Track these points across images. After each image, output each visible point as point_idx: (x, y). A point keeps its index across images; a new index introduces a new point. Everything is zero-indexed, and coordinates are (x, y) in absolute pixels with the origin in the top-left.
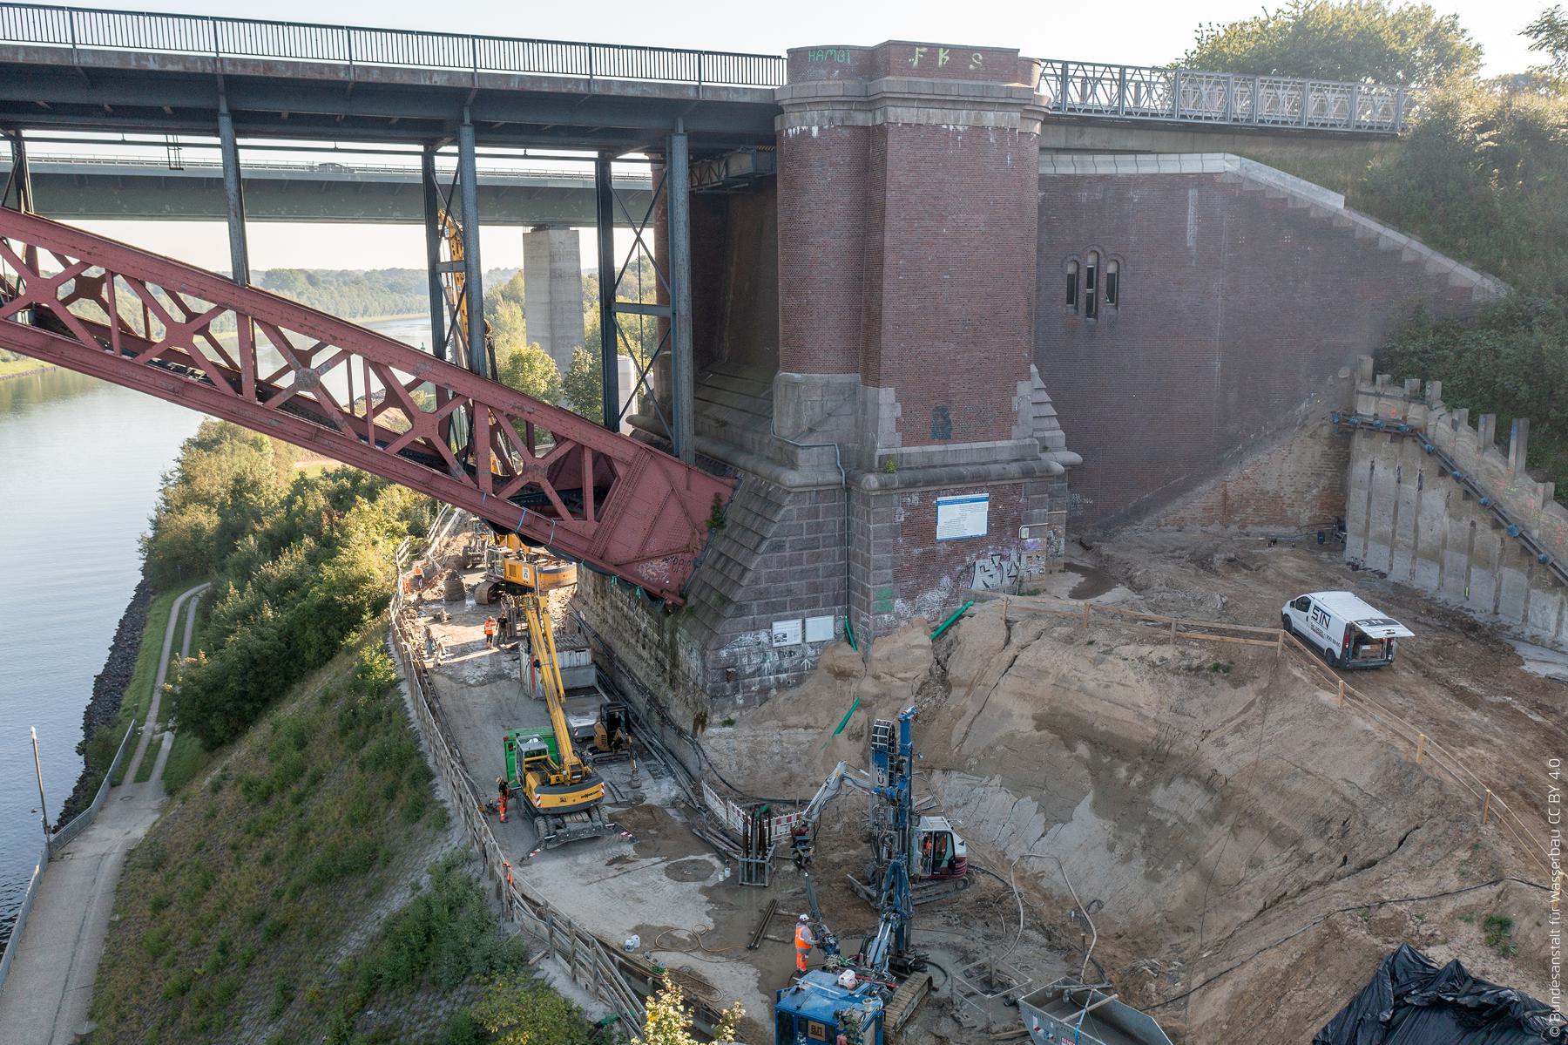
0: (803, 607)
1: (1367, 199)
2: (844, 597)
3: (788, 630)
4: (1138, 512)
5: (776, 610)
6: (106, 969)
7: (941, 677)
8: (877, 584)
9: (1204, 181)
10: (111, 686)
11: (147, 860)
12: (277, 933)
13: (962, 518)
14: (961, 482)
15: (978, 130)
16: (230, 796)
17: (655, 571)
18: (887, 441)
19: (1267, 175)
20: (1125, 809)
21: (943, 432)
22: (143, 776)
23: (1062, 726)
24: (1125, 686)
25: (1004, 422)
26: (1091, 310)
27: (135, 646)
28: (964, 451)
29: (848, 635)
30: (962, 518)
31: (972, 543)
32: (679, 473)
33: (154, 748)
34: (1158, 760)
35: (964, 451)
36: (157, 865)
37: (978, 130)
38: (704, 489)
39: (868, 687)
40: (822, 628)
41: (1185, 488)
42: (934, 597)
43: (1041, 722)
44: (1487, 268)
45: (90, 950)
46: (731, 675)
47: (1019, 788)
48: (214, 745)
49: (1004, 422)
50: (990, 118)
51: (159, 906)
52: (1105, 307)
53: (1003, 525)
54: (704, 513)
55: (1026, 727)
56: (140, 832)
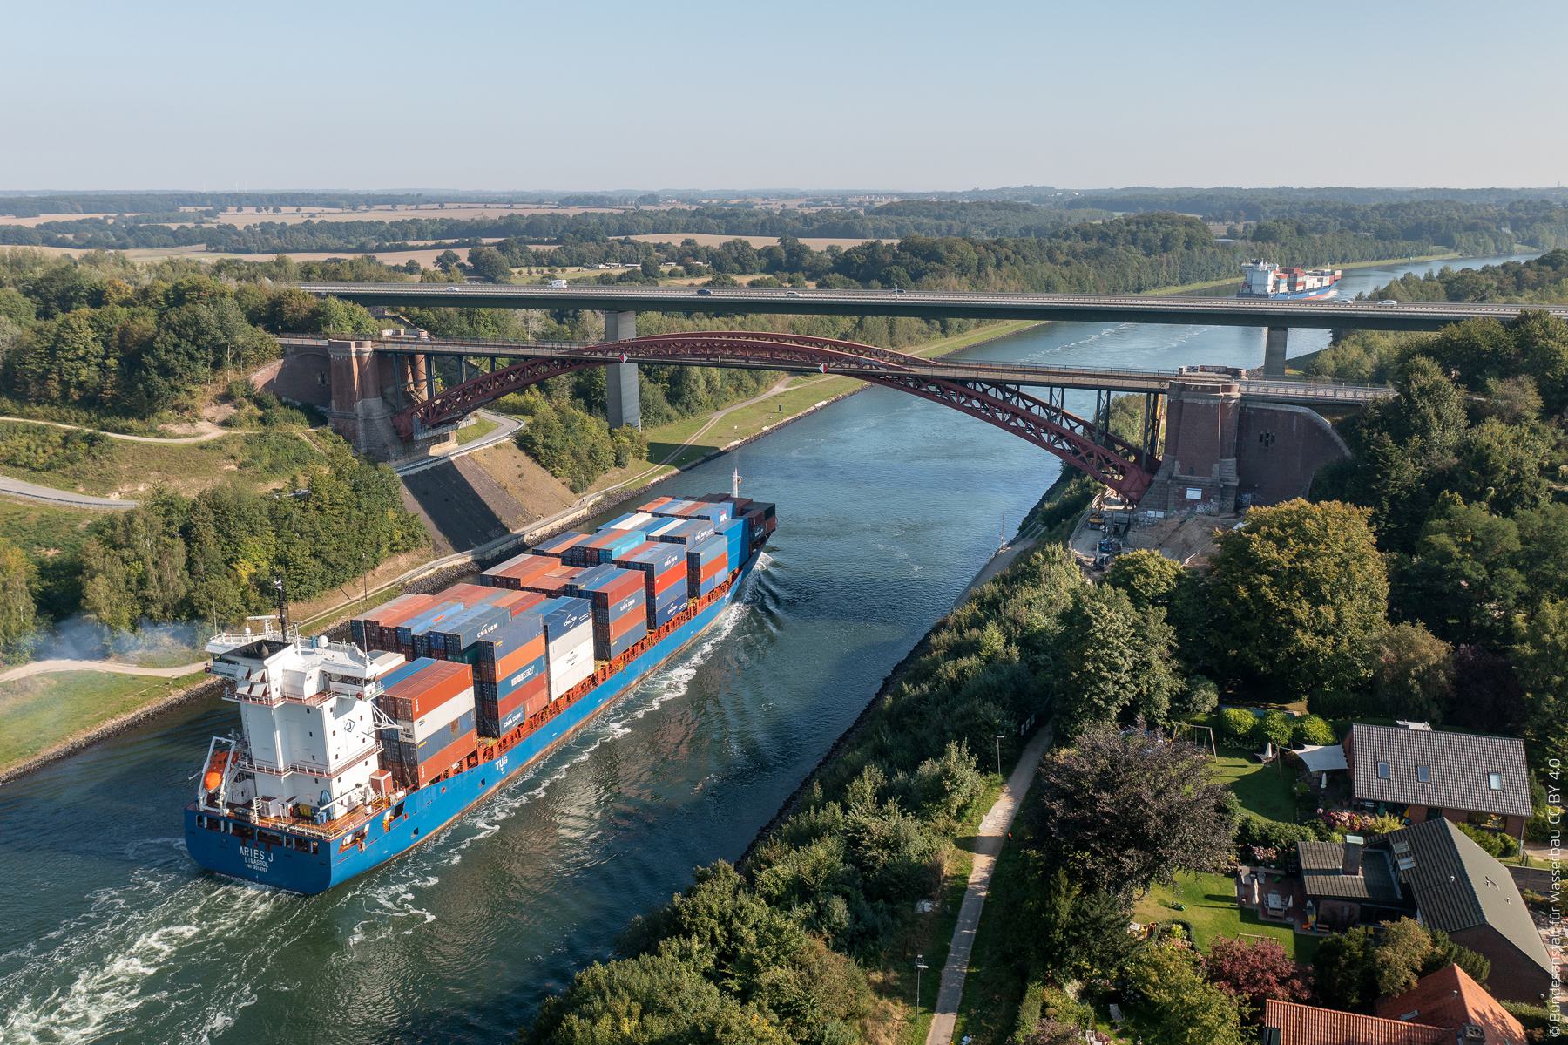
2: (1165, 509)
3: (1151, 513)
8: (1171, 506)
10: (1033, 512)
13: (1194, 494)
14: (1195, 486)
15: (1208, 405)
17: (1133, 494)
19: (1315, 415)
21: (1192, 472)
28: (1197, 478)
29: (1166, 518)
30: (1194, 494)
35: (1197, 478)
37: (1208, 405)
38: (1147, 477)
40: (1160, 514)
53: (1205, 498)
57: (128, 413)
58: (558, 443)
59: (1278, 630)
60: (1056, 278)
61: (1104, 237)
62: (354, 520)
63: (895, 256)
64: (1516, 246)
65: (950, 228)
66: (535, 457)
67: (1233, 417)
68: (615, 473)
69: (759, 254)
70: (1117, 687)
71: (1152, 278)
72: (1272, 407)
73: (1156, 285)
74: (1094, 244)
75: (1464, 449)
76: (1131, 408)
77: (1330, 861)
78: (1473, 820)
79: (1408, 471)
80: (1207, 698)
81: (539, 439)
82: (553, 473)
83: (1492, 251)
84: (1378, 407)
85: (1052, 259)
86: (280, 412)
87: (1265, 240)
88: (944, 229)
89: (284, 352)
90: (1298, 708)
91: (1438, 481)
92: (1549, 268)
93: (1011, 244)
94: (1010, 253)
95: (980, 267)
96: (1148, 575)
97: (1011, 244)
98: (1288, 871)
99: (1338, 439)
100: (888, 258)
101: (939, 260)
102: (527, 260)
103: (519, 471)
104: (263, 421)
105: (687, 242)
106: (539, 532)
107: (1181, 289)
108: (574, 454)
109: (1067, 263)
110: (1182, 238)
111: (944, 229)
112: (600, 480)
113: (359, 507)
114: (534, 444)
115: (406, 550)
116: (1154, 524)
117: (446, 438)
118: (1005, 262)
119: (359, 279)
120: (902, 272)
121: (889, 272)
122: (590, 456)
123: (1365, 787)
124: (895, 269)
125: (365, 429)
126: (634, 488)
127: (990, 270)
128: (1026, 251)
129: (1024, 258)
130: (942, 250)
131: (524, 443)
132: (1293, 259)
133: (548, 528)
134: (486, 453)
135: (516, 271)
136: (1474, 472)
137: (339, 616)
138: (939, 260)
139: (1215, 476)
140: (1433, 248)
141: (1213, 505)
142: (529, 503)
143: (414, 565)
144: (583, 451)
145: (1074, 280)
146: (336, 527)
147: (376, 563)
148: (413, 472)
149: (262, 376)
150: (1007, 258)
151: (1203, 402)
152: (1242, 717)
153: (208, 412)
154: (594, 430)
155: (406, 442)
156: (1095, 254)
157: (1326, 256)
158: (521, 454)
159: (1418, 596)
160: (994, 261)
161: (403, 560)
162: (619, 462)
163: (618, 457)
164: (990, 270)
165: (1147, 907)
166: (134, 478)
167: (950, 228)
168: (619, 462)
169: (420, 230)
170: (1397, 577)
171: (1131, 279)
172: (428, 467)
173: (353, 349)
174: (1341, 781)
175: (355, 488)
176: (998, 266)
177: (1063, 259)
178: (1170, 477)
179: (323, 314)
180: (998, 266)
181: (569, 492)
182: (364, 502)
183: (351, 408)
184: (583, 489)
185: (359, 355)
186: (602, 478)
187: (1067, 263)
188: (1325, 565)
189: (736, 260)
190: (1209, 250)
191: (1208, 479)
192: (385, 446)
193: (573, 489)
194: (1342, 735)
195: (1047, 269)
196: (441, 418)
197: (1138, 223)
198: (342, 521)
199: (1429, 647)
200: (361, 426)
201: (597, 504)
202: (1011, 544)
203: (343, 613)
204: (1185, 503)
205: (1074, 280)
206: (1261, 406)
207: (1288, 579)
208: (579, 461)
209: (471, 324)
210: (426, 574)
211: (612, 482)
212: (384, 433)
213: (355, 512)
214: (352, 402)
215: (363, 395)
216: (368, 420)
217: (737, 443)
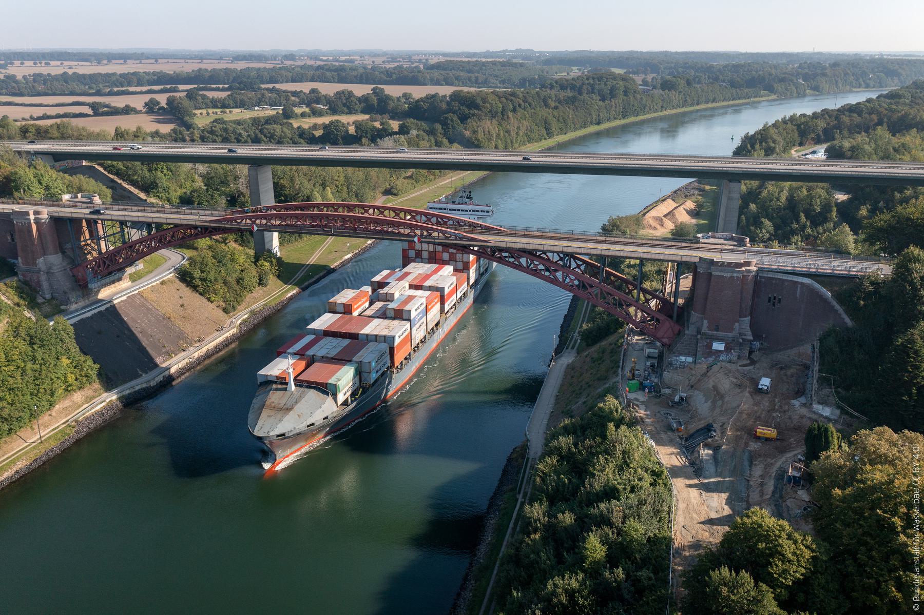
0: (687, 355)
1: (838, 297)
2: (695, 355)
3: (683, 358)
4: (780, 350)
5: (681, 354)
6: (562, 385)
7: (705, 375)
9: (802, 284)
11: (571, 368)
12: (589, 386)
13: (718, 346)
14: (719, 340)
16: (588, 359)
17: (665, 340)
18: (705, 329)
19: (817, 285)
20: (714, 402)
21: (717, 330)
22: (573, 348)
23: (715, 388)
24: (725, 384)
25: (731, 330)
26: (774, 304)
27: (576, 307)
28: (721, 334)
29: (695, 362)
30: (718, 346)
31: (720, 351)
32: (672, 324)
33: (576, 341)
34: (722, 397)
36: (573, 369)
37: (732, 277)
39: (694, 372)
40: (690, 359)
41: (792, 348)
42: (711, 359)
43: (713, 387)
44: (852, 320)
45: (559, 382)
46: (671, 364)
47: (705, 395)
48: (589, 346)
49: (731, 330)
50: (735, 275)
51: (572, 377)
52: (778, 306)
53: (728, 349)
54: (676, 332)
55: (711, 386)
56: (570, 361)
58: (212, 276)
60: (550, 117)
61: (573, 87)
62: (29, 372)
63: (448, 104)
64: (808, 91)
65: (477, 78)
66: (194, 288)
67: (751, 287)
68: (258, 291)
69: (360, 100)
71: (607, 115)
72: (780, 276)
73: (609, 120)
74: (569, 93)
76: (622, 228)
81: (197, 274)
82: (209, 299)
84: (872, 283)
85: (547, 105)
88: (473, 79)
92: (855, 115)
93: (521, 95)
94: (521, 102)
95: (503, 112)
96: (784, 559)
97: (521, 95)
99: (837, 307)
100: (444, 106)
101: (477, 107)
102: (206, 104)
103: (181, 302)
105: (313, 91)
106: (196, 355)
107: (623, 122)
108: (225, 282)
109: (556, 108)
110: (622, 89)
111: (473, 79)
112: (247, 299)
113: (34, 359)
114: (193, 278)
115: (80, 388)
116: (684, 366)
117: (120, 279)
118: (518, 109)
119: (64, 137)
120: (455, 118)
121: (446, 118)
122: (238, 282)
124: (450, 115)
125: (48, 280)
126: (273, 304)
127: (510, 114)
128: (530, 100)
129: (530, 104)
130: (479, 101)
131: (184, 276)
132: (686, 101)
133: (204, 350)
134: (153, 290)
135: (198, 112)
137: (14, 462)
138: (477, 107)
139: (735, 333)
140: (762, 92)
141: (734, 354)
142: (189, 329)
143: (89, 399)
144: (232, 280)
145: (561, 119)
146: (11, 381)
147: (52, 405)
148: (89, 314)
150: (520, 105)
151: (729, 275)
154: (242, 259)
155: (83, 287)
156: (571, 101)
157: (704, 99)
158: (182, 286)
160: (511, 107)
161: (78, 396)
162: (261, 282)
163: (260, 280)
164: (510, 114)
167: (477, 78)
168: (261, 282)
171: (594, 117)
172: (103, 308)
173: (32, 217)
175: (31, 344)
176: (514, 110)
177: (553, 104)
178: (699, 332)
179: (14, 181)
180: (514, 110)
181: (222, 314)
182: (39, 354)
183: (35, 264)
184: (234, 309)
185: (37, 221)
186: (249, 297)
187: (556, 108)
189: (344, 105)
190: (638, 97)
191: (730, 335)
192: (65, 293)
193: (225, 311)
195: (544, 112)
196: (111, 267)
197: (593, 79)
198: (18, 375)
200: (43, 278)
201: (244, 321)
202: (559, 351)
203: (18, 459)
204: (710, 352)
205: (561, 119)
206: (770, 275)
208: (230, 288)
209: (150, 171)
210: (98, 408)
211: (256, 300)
212: (63, 282)
213: (29, 365)
214: (34, 259)
215: (45, 253)
216: (49, 273)
217: (349, 256)
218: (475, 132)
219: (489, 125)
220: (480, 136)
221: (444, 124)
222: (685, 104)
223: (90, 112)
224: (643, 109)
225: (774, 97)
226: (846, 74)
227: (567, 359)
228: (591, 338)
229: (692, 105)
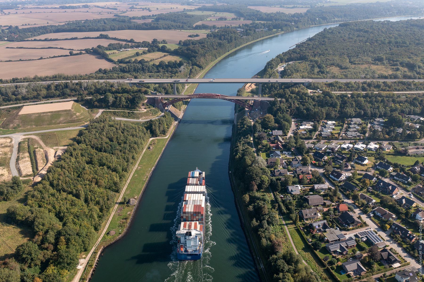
57: (133, 108)
59: (267, 125)
64: (295, 28)
65: (179, 26)
70: (258, 130)
73: (231, 49)
75: (279, 106)
77: (272, 138)
78: (279, 135)
79: (275, 109)
80: (263, 130)
83: (290, 31)
86: (150, 106)
87: (248, 35)
89: (148, 98)
90: (269, 130)
91: (278, 110)
98: (270, 139)
104: (149, 107)
111: (178, 26)
123: (274, 134)
136: (280, 109)
149: (146, 101)
152: (266, 131)
153: (142, 107)
159: (277, 121)
165: (263, 141)
166: (142, 117)
167: (179, 26)
169: (50, 30)
170: (275, 120)
174: (272, 134)
187: (216, 49)
188: (270, 120)
194: (272, 131)
199: (277, 125)
202: (235, 113)
207: (268, 121)
218: (200, 62)
219: (202, 60)
220: (201, 63)
221: (191, 61)
222: (254, 39)
223: (69, 54)
224: (241, 44)
225: (283, 32)
226: (308, 21)
227: (237, 114)
228: (240, 111)
229: (256, 39)
